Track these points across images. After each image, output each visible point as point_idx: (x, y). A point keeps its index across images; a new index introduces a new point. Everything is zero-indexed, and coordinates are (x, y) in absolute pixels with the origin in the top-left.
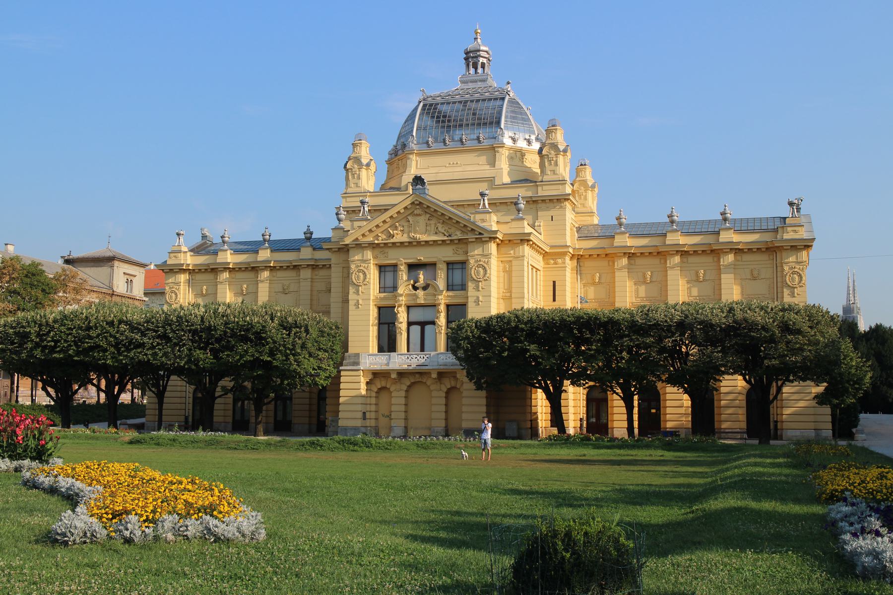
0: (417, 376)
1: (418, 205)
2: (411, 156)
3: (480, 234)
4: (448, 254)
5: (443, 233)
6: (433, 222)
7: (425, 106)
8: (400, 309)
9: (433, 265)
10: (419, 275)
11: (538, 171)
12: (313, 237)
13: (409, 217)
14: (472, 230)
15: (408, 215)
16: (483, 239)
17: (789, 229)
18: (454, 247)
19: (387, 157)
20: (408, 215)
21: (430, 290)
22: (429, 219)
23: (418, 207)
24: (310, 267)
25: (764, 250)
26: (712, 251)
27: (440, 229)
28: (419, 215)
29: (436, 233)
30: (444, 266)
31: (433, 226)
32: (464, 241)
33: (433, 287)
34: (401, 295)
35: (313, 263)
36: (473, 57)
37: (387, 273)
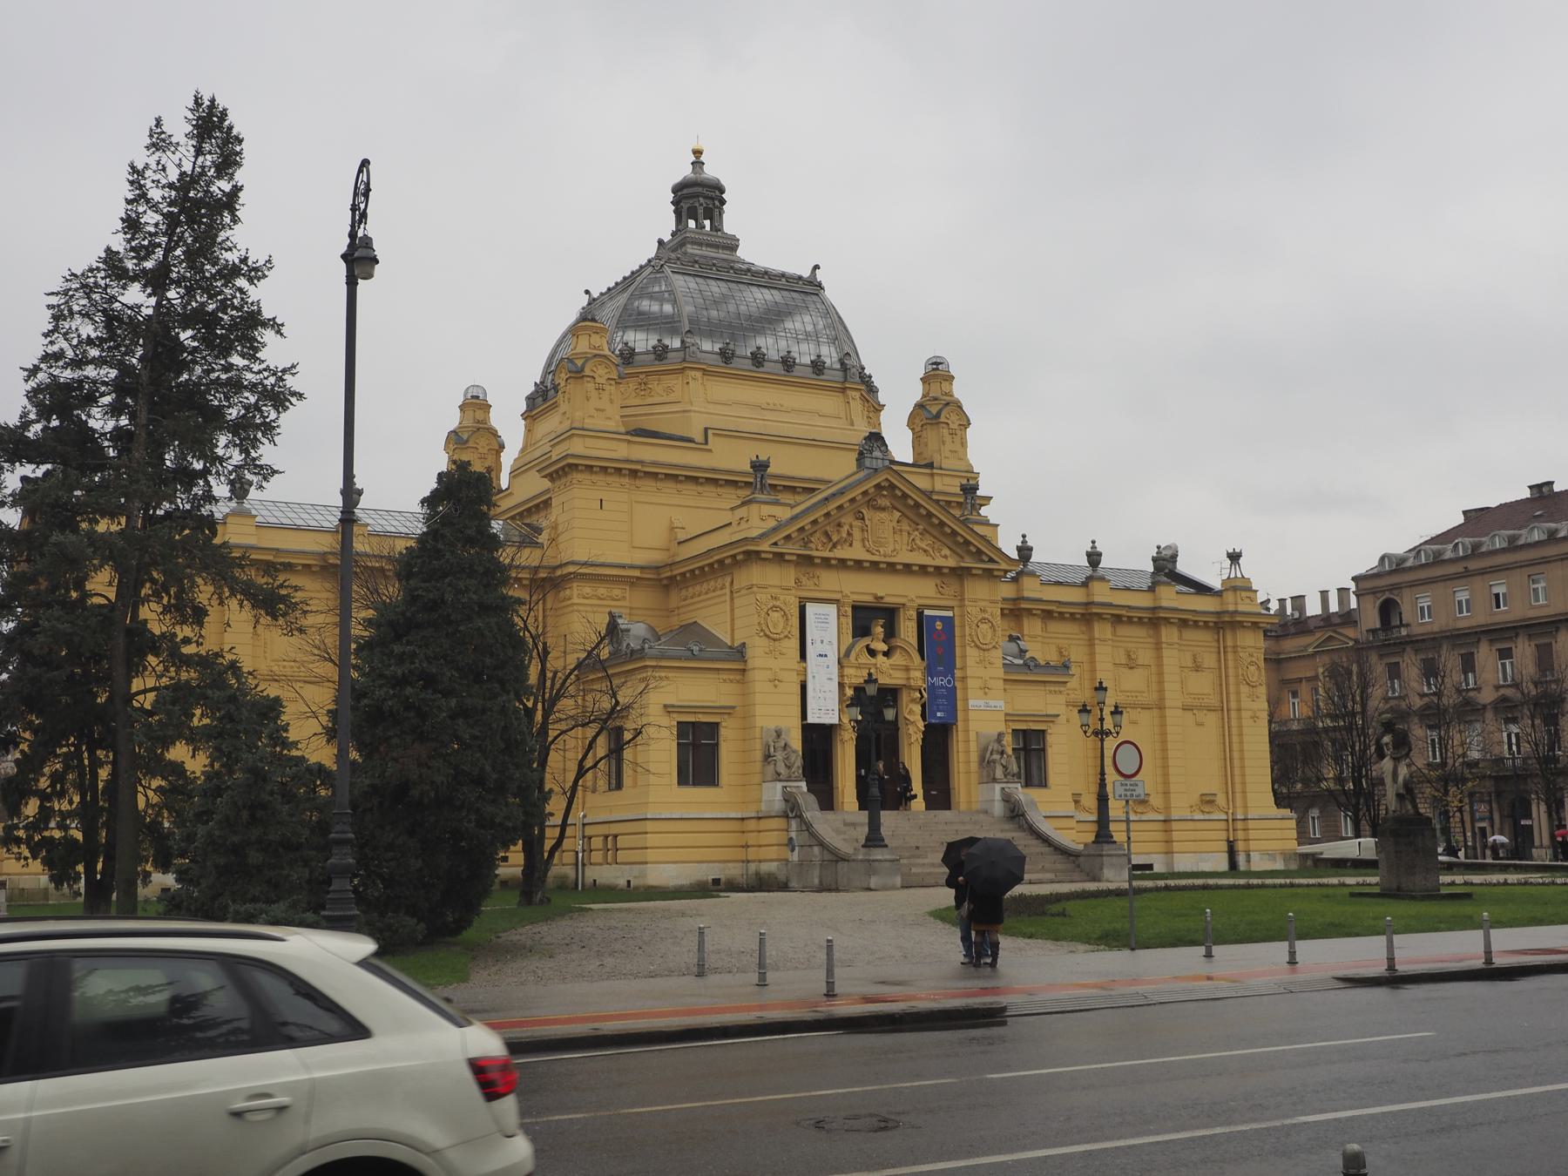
1: (883, 488)
3: (991, 560)
5: (925, 551)
14: (979, 552)
18: (939, 582)
23: (885, 493)
27: (918, 542)
28: (883, 509)
31: (905, 534)
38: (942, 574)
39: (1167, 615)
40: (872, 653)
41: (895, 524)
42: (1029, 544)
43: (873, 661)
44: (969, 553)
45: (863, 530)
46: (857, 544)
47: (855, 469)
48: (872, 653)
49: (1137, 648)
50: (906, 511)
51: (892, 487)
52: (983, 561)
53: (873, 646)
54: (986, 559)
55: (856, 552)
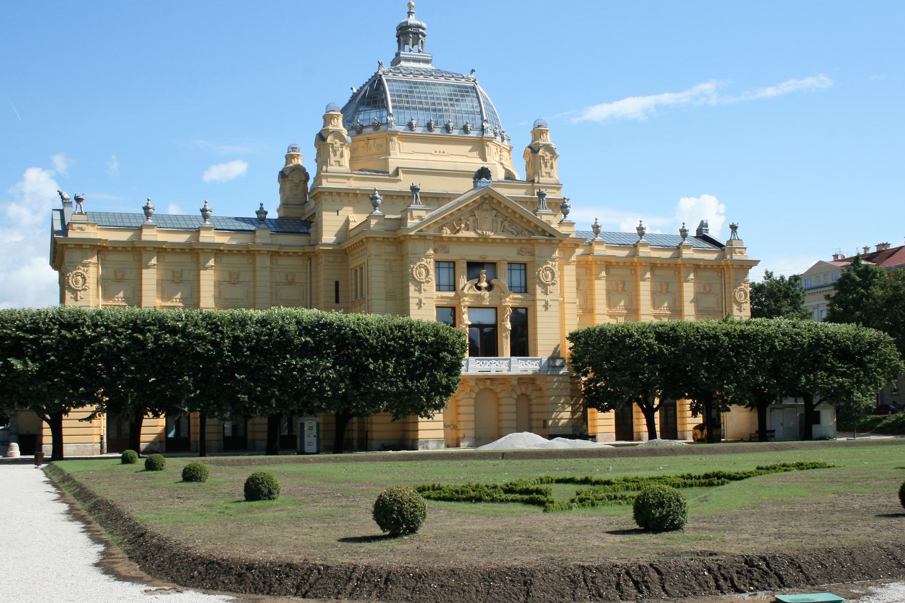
0: (488, 382)
3: (551, 235)
4: (511, 254)
5: (511, 232)
9: (494, 264)
12: (268, 217)
13: (475, 212)
16: (554, 242)
27: (507, 226)
28: (487, 210)
30: (506, 267)
31: (499, 223)
32: (532, 242)
33: (499, 287)
34: (466, 295)
35: (276, 250)
36: (413, 33)
37: (447, 270)
40: (479, 288)
41: (493, 217)
43: (479, 292)
44: (538, 231)
45: (475, 222)
47: (473, 187)
48: (479, 288)
49: (668, 283)
50: (499, 209)
53: (479, 285)
54: (548, 235)
55: (471, 234)
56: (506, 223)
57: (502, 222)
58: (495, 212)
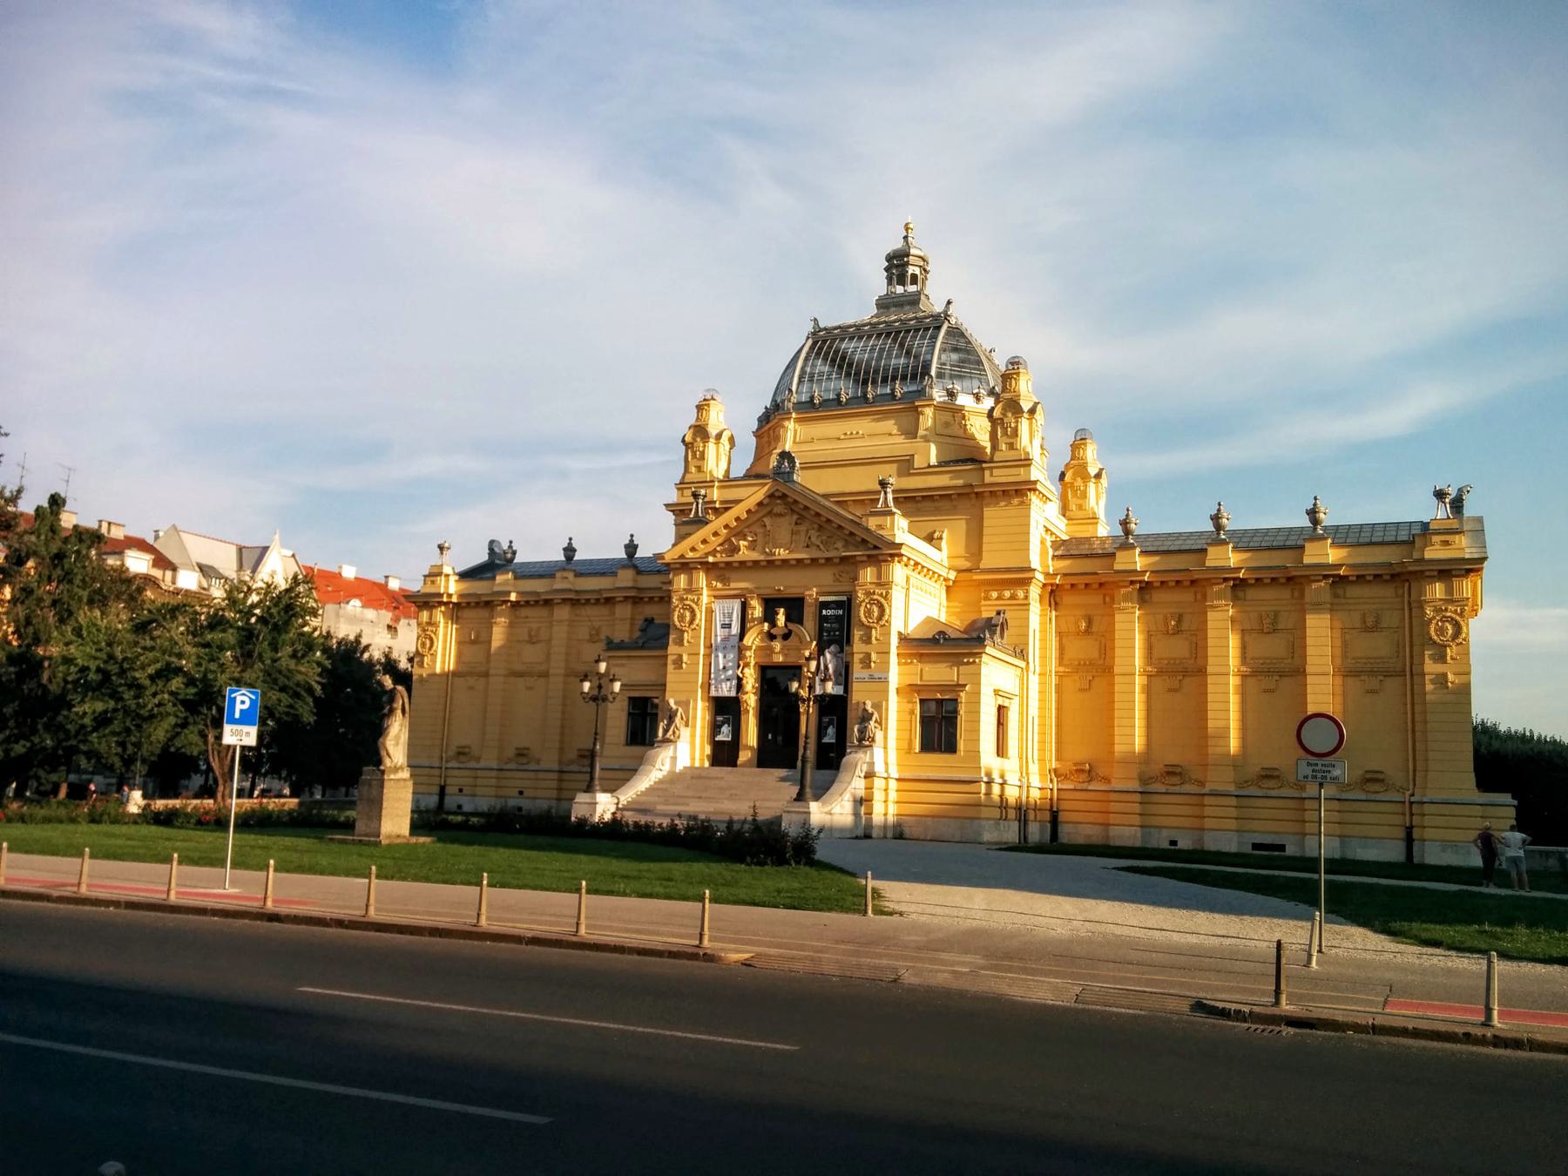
1: (779, 498)
2: (786, 423)
3: (876, 547)
6: (803, 528)
7: (815, 343)
8: (746, 670)
10: (778, 614)
11: (987, 445)
13: (765, 519)
14: (864, 541)
15: (764, 516)
16: (881, 558)
17: (1436, 539)
19: (755, 426)
20: (764, 516)
21: (793, 640)
22: (796, 524)
23: (779, 501)
24: (631, 600)
25: (1388, 577)
26: (1289, 579)
27: (813, 539)
28: (781, 515)
29: (808, 546)
31: (803, 534)
33: (797, 635)
38: (835, 564)
39: (1308, 573)
42: (635, 543)
46: (759, 547)
51: (784, 496)
52: (869, 549)
56: (814, 534)
57: (807, 531)
58: (795, 517)
